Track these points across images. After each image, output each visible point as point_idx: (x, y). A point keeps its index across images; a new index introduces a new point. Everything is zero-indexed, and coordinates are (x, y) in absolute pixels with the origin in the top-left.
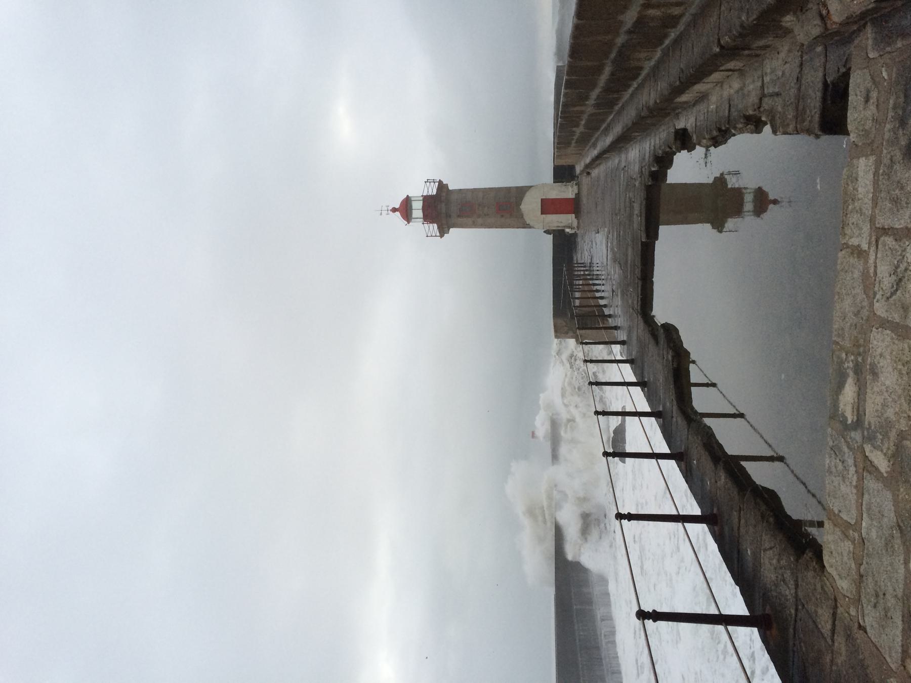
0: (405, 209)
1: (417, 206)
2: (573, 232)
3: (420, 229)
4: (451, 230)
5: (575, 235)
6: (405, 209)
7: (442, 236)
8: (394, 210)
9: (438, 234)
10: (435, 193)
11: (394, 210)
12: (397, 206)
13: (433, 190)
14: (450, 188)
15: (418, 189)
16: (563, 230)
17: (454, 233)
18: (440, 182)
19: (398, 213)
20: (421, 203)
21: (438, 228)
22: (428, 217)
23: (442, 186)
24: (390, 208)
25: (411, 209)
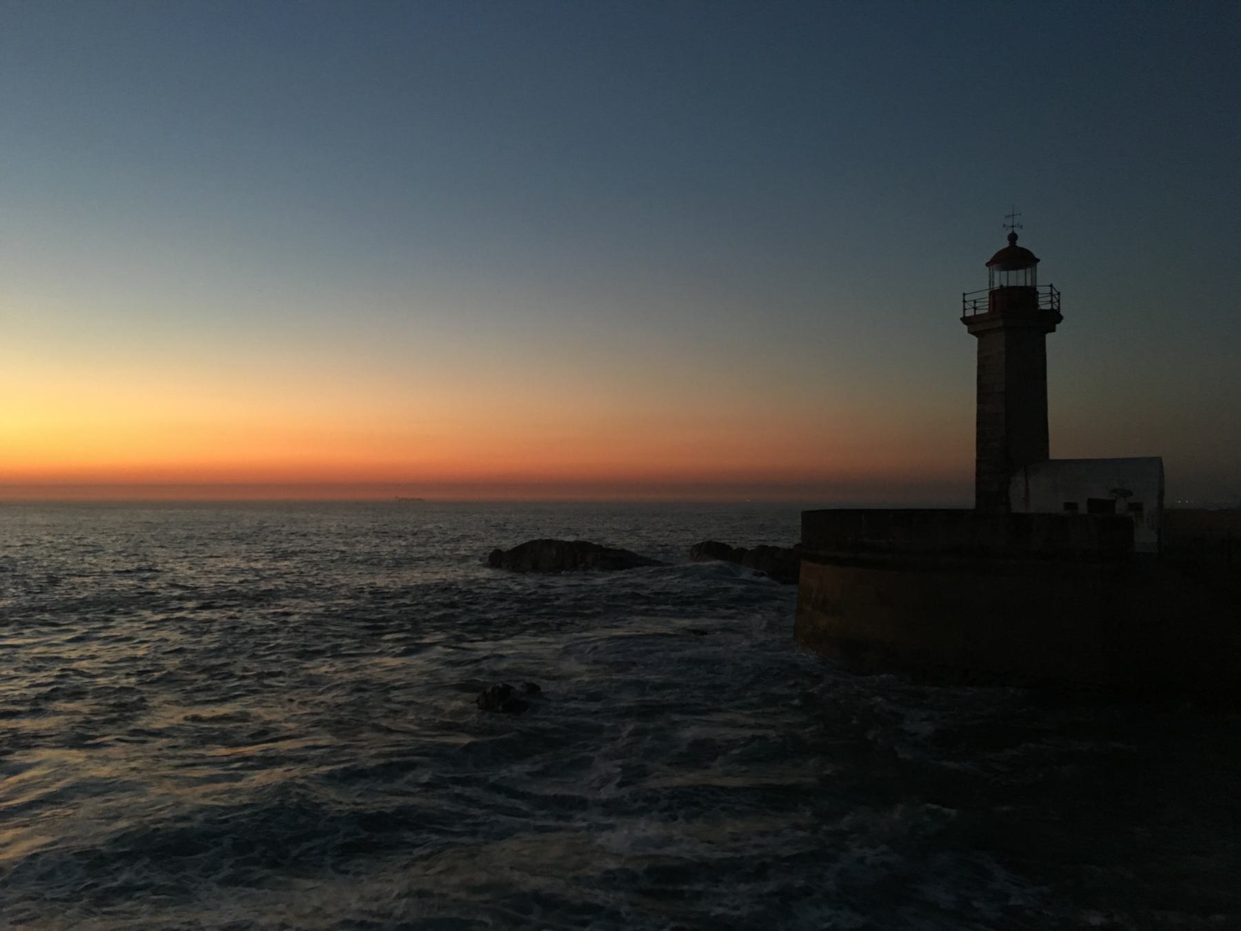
0: (1015, 257)
1: (1017, 278)
6: (1015, 257)
7: (965, 320)
8: (1013, 238)
9: (970, 313)
10: (1043, 307)
11: (1013, 238)
12: (1019, 243)
13: (1044, 305)
14: (1049, 337)
18: (1059, 318)
19: (1006, 244)
22: (997, 296)
23: (1053, 318)
24: (1017, 231)
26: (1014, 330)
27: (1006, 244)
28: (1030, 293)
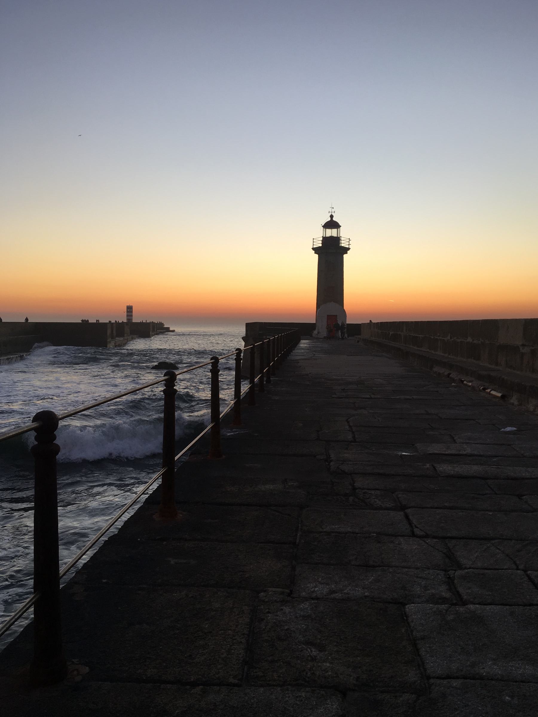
0: (332, 224)
2: (314, 335)
3: (317, 235)
4: (317, 255)
5: (311, 336)
6: (332, 224)
7: (313, 249)
8: (332, 216)
10: (342, 245)
11: (332, 216)
12: (334, 219)
13: (344, 244)
14: (345, 256)
15: (345, 235)
16: (315, 329)
17: (315, 258)
18: (349, 249)
20: (335, 235)
21: (320, 247)
22: (325, 240)
23: (346, 250)
24: (333, 214)
25: (332, 228)
26: (331, 254)
27: (329, 219)
28: (337, 240)
